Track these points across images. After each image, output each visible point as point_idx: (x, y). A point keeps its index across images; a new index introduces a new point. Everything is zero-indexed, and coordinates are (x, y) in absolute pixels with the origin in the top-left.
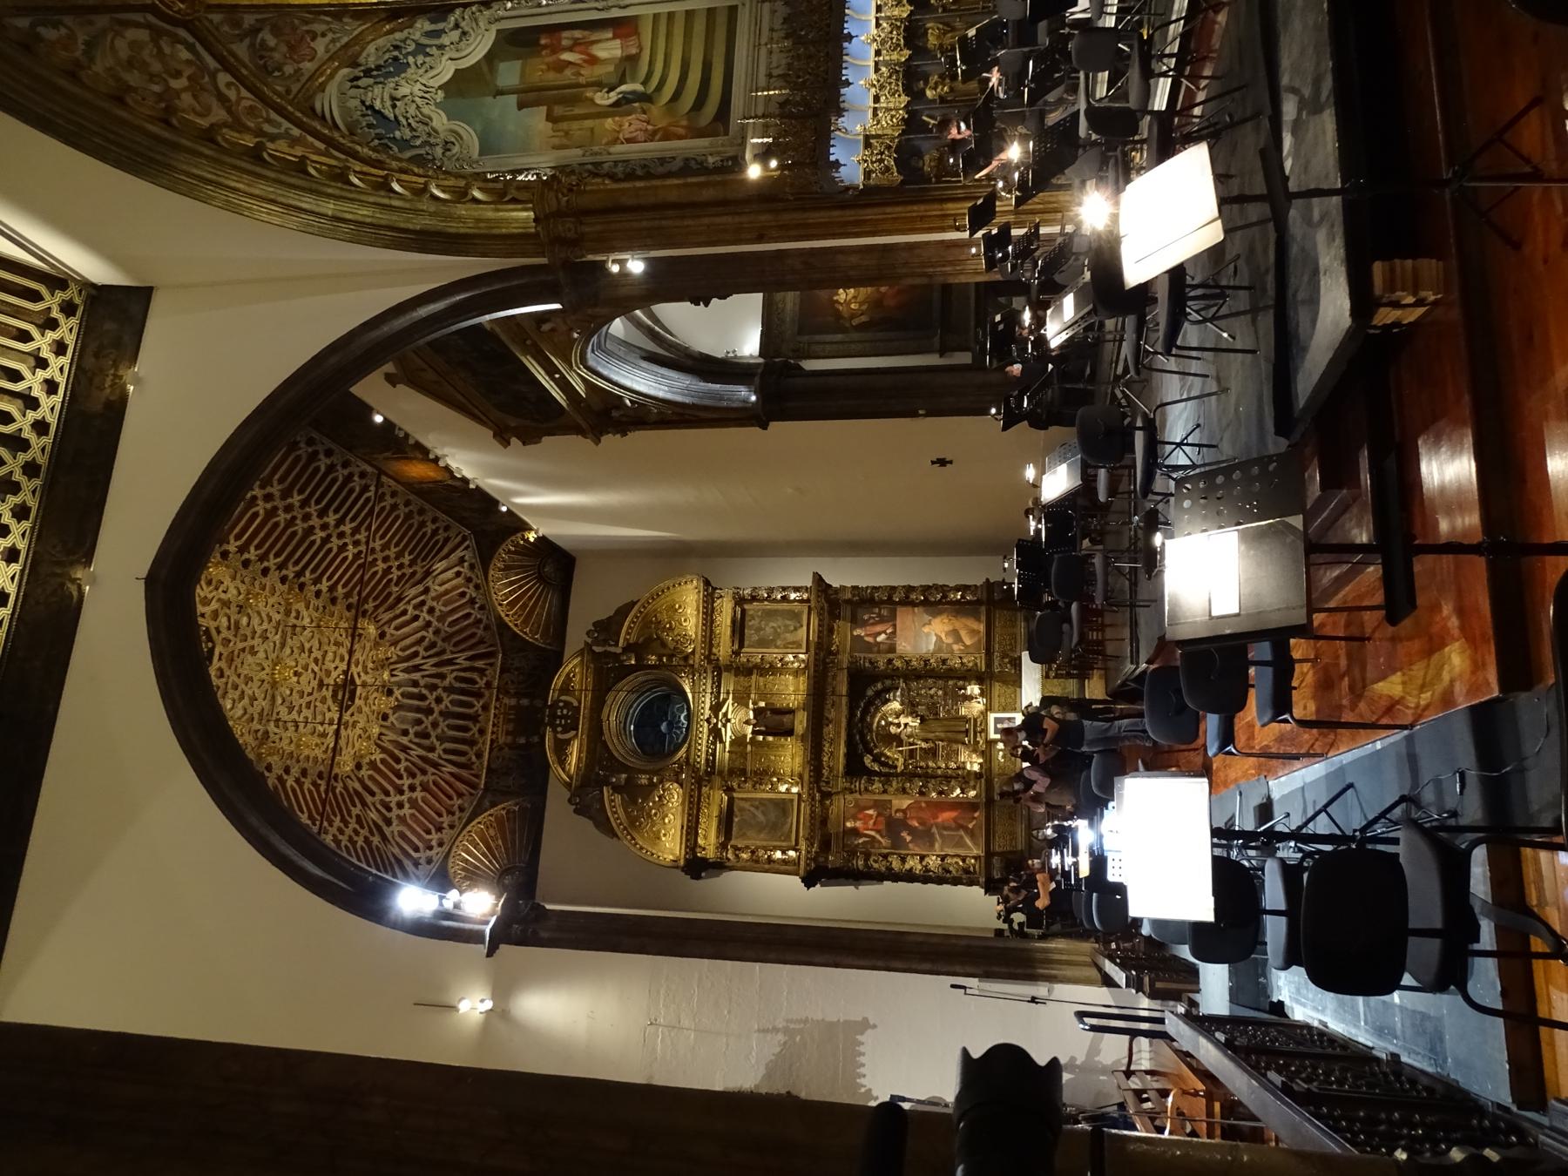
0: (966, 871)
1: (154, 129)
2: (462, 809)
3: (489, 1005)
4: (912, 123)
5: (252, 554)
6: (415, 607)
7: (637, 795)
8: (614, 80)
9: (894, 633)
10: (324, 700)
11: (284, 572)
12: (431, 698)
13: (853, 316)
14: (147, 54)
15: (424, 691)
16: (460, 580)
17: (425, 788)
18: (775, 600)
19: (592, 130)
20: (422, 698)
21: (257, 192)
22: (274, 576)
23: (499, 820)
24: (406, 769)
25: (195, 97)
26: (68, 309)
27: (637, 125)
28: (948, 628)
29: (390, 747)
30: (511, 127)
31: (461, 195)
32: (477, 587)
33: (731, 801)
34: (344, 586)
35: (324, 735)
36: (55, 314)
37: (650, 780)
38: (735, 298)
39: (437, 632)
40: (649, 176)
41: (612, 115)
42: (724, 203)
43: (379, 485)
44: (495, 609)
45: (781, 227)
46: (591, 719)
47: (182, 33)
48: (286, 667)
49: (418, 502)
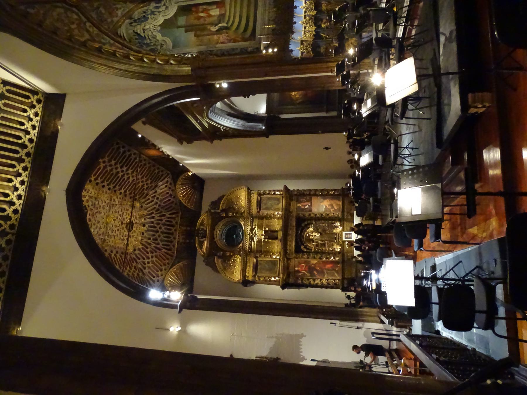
0: (335, 284)
1: (67, 42)
2: (168, 264)
3: (180, 329)
4: (317, 36)
5: (99, 181)
8: (217, 22)
9: (311, 205)
10: (123, 229)
11: (110, 187)
12: (158, 227)
13: (297, 99)
15: (156, 225)
17: (156, 257)
18: (271, 194)
19: (210, 39)
20: (155, 227)
21: (99, 62)
23: (181, 268)
24: (150, 251)
26: (39, 101)
28: (329, 203)
29: (145, 243)
31: (167, 62)
32: (172, 191)
33: (257, 261)
35: (123, 240)
36: (35, 103)
38: (257, 96)
39: (159, 206)
40: (230, 55)
41: (216, 34)
43: (140, 157)
44: (178, 198)
47: (75, 9)
48: (111, 218)
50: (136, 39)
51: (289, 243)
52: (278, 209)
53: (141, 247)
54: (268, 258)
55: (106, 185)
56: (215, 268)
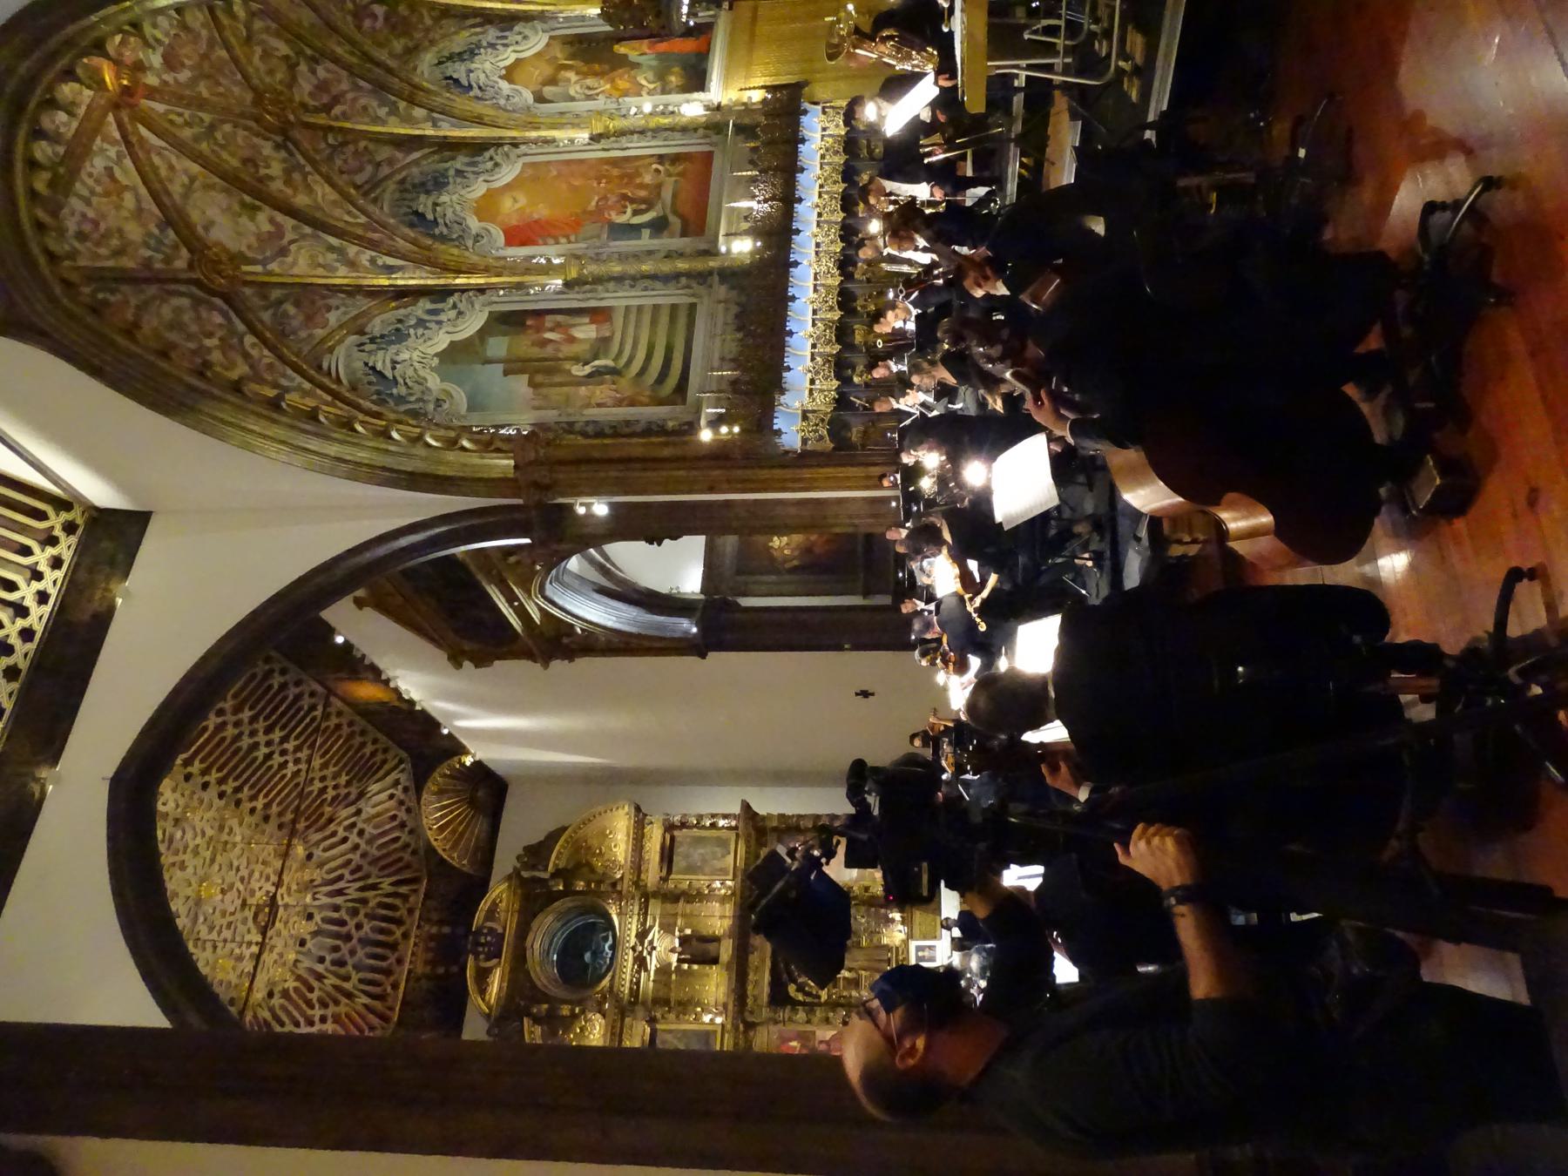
4: (842, 402)
6: (346, 829)
8: (588, 356)
11: (223, 787)
12: (352, 923)
13: (786, 559)
14: (187, 317)
15: (346, 918)
16: (392, 803)
18: (704, 827)
22: (213, 792)
25: (224, 354)
26: (70, 528)
29: (305, 975)
32: (409, 811)
33: (654, 1033)
34: (280, 804)
35: (240, 958)
36: (58, 532)
37: (572, 1011)
39: (364, 855)
42: (683, 459)
43: (327, 705)
45: (729, 481)
46: (516, 948)
47: (218, 301)
49: (361, 723)
51: (751, 977)
52: (724, 871)
53: (291, 984)
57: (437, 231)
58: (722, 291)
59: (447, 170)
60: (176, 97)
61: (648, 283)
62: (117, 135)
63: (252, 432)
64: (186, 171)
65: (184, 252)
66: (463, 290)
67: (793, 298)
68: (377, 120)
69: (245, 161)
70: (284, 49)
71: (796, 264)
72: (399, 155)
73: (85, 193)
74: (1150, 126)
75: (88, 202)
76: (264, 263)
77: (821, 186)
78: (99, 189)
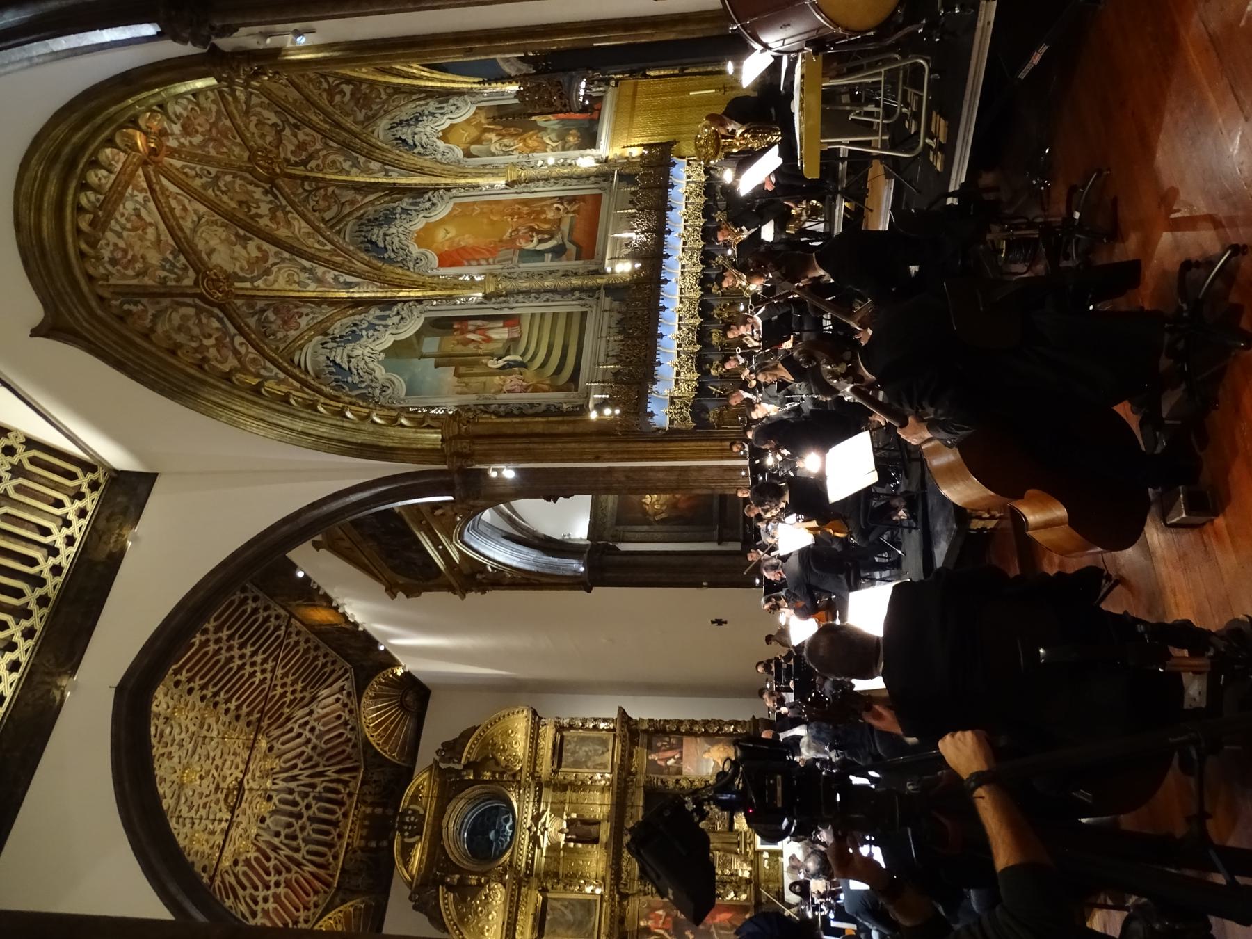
1: (192, 371)
4: (701, 390)
7: (466, 893)
8: (502, 353)
9: (681, 758)
11: (205, 692)
12: (303, 804)
13: (656, 514)
15: (298, 799)
16: (339, 705)
17: (288, 885)
18: (588, 729)
20: (295, 804)
22: (196, 695)
23: (347, 916)
24: (275, 867)
25: (219, 351)
26: (94, 486)
27: (516, 381)
29: (264, 846)
30: (428, 379)
32: (351, 711)
34: (248, 706)
35: (213, 833)
36: (84, 489)
37: (479, 880)
38: (576, 498)
39: (314, 748)
40: (522, 415)
41: (499, 375)
42: (573, 435)
43: (289, 625)
46: (433, 827)
47: (216, 311)
48: (193, 771)
50: (331, 373)
53: (253, 854)
54: (572, 892)
55: (197, 687)
56: (437, 920)
57: (386, 256)
58: (607, 302)
59: (394, 209)
60: (191, 157)
61: (548, 295)
62: (145, 185)
63: (237, 411)
64: (196, 212)
65: (191, 273)
66: (405, 301)
67: (664, 308)
68: (341, 171)
69: (240, 203)
70: (274, 119)
71: (666, 281)
72: (359, 198)
73: (118, 228)
74: (953, 194)
75: (120, 236)
76: (252, 280)
77: (686, 221)
78: (129, 226)
